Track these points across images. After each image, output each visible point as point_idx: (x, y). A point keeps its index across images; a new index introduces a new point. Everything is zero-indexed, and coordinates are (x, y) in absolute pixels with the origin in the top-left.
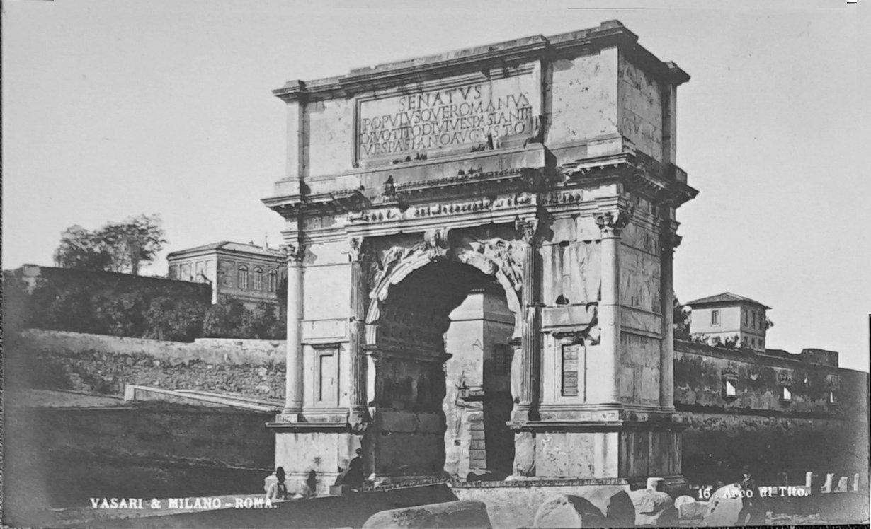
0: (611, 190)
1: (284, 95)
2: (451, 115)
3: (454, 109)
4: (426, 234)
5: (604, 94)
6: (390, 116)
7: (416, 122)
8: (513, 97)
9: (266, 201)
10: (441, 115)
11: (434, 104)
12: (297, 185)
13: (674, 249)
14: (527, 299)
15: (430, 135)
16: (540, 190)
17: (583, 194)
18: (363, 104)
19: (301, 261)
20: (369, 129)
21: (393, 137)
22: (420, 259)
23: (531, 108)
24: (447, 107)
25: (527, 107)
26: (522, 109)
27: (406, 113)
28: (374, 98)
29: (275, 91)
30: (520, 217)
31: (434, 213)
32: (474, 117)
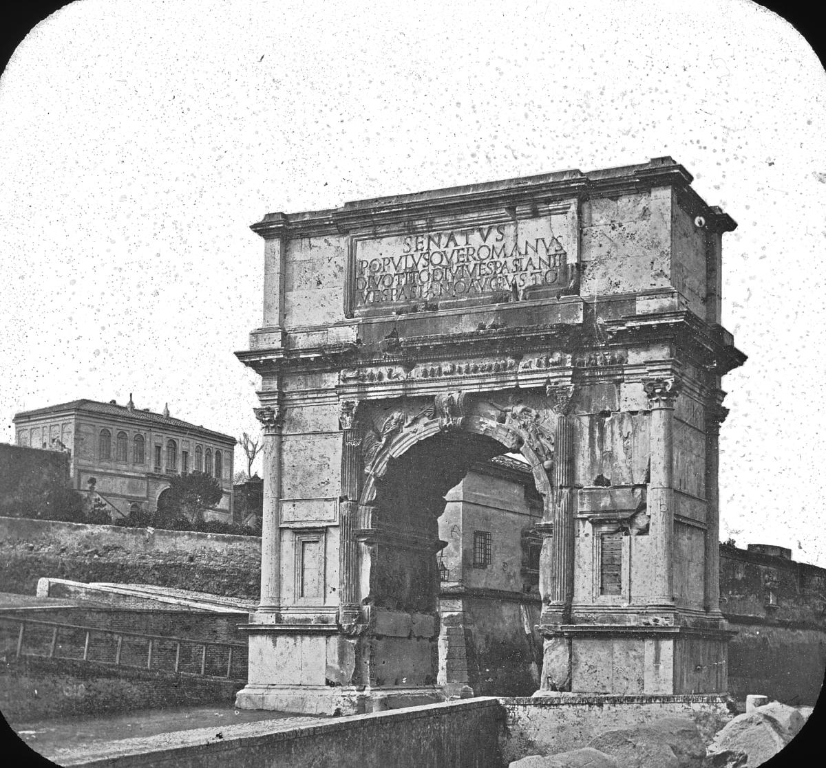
0: (660, 353)
2: (468, 259)
3: (471, 252)
4: (436, 398)
6: (392, 258)
7: (424, 266)
8: (543, 241)
9: (240, 355)
10: (455, 259)
11: (447, 246)
12: (279, 336)
14: (560, 479)
15: (441, 282)
16: (577, 350)
17: (627, 356)
18: (359, 243)
19: (281, 428)
20: (367, 273)
21: (395, 283)
22: (424, 429)
23: (565, 253)
24: (463, 249)
25: (559, 252)
26: (556, 255)
27: (412, 256)
30: (552, 380)
31: (446, 373)
32: (496, 263)
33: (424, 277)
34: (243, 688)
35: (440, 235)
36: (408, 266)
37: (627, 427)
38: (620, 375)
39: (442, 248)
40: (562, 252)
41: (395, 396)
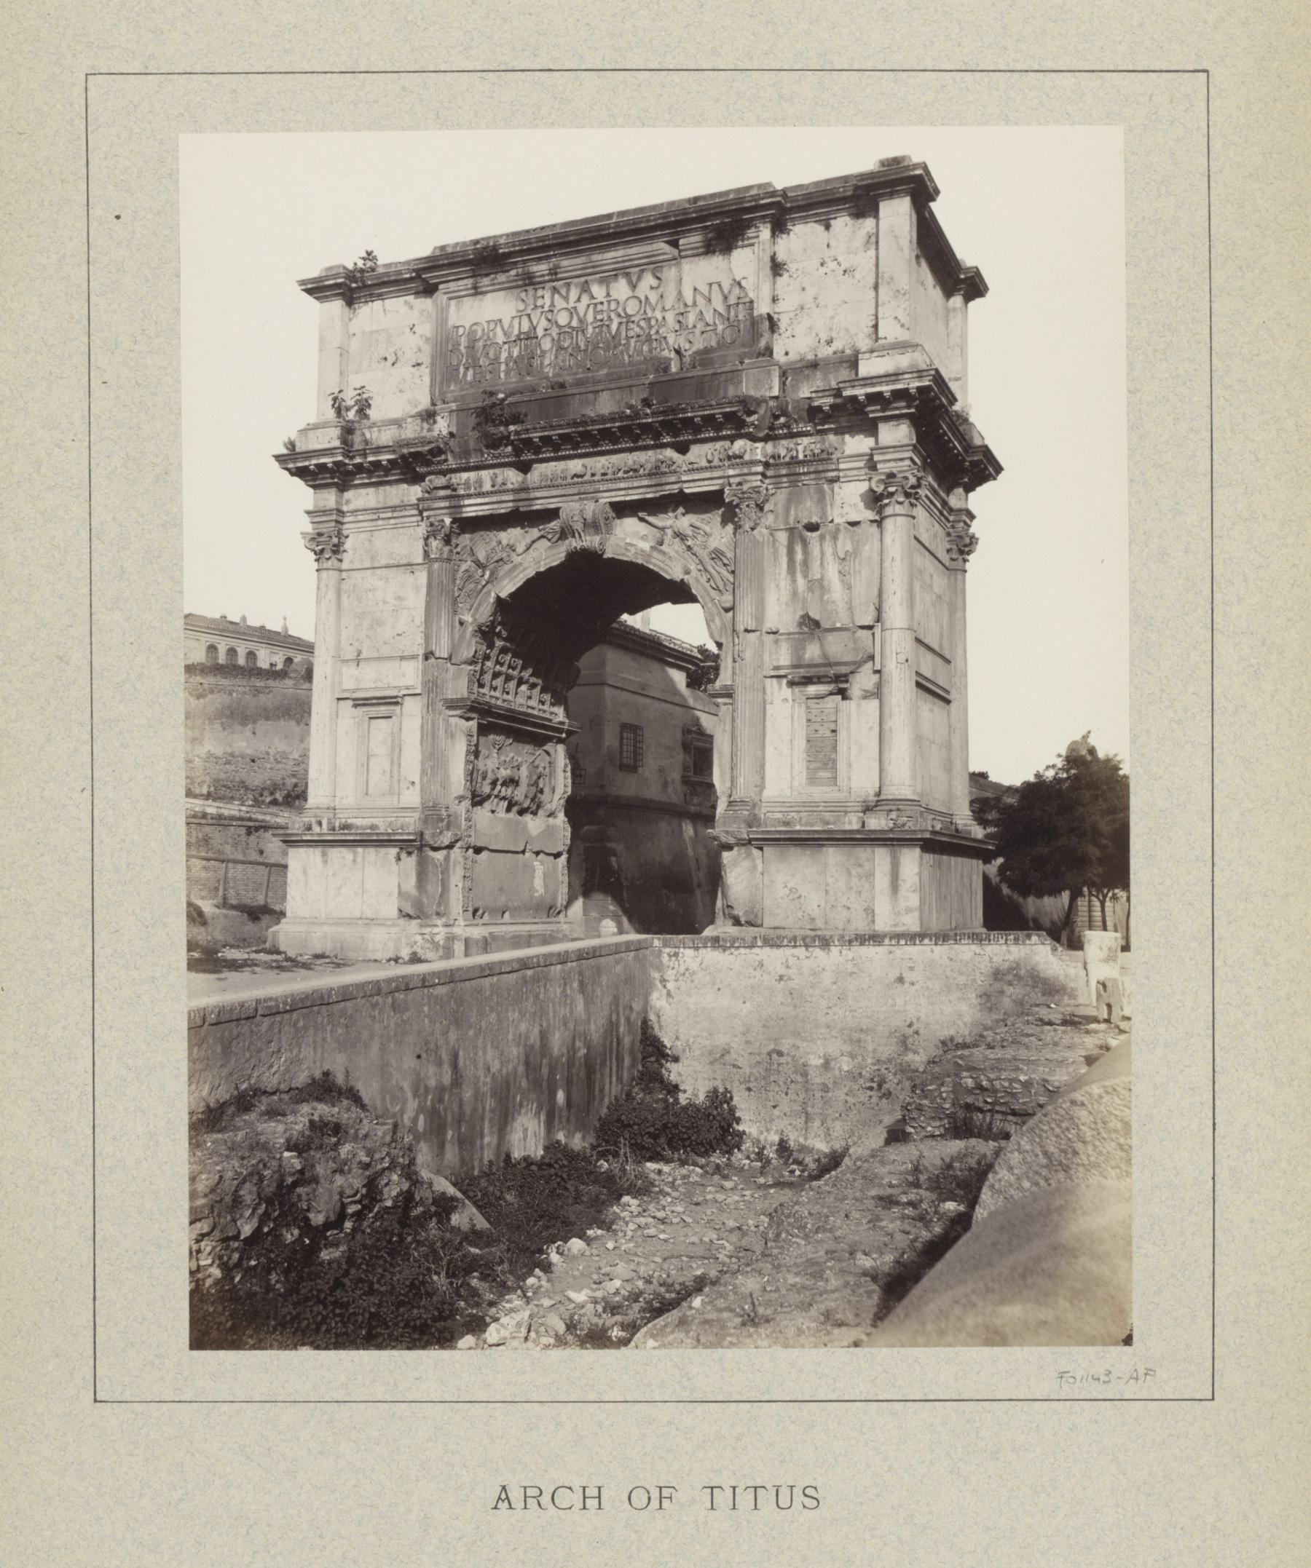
1: (317, 289)
3: (613, 306)
5: (886, 276)
6: (500, 321)
8: (720, 285)
10: (590, 318)
11: (579, 300)
18: (453, 303)
19: (340, 560)
23: (752, 302)
24: (602, 303)
26: (737, 304)
27: (529, 316)
28: (472, 291)
29: (302, 283)
30: (732, 480)
32: (649, 319)
35: (568, 285)
37: (845, 544)
39: (572, 304)
40: (747, 300)
41: (503, 511)
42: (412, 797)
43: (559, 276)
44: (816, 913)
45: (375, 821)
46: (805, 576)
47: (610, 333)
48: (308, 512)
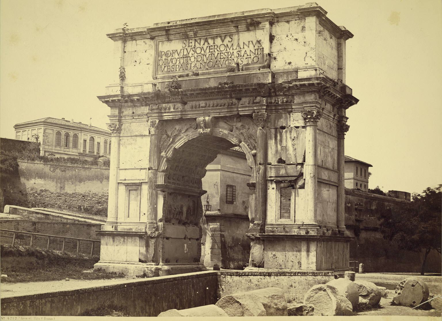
0: (310, 98)
1: (112, 36)
2: (214, 51)
6: (177, 51)
9: (100, 98)
11: (204, 44)
12: (119, 88)
13: (345, 133)
15: (201, 62)
19: (120, 133)
21: (178, 62)
23: (263, 48)
24: (212, 46)
25: (260, 48)
26: (258, 49)
27: (187, 49)
29: (108, 35)
30: (256, 111)
31: (202, 107)
33: (193, 59)
34: (97, 262)
35: (200, 39)
36: (184, 54)
37: (294, 134)
38: (290, 108)
39: (201, 46)
40: (261, 48)
41: (177, 118)
42: (145, 219)
43: (197, 36)
44: (281, 263)
45: (131, 227)
46: (281, 145)
47: (215, 57)
48: (108, 116)
